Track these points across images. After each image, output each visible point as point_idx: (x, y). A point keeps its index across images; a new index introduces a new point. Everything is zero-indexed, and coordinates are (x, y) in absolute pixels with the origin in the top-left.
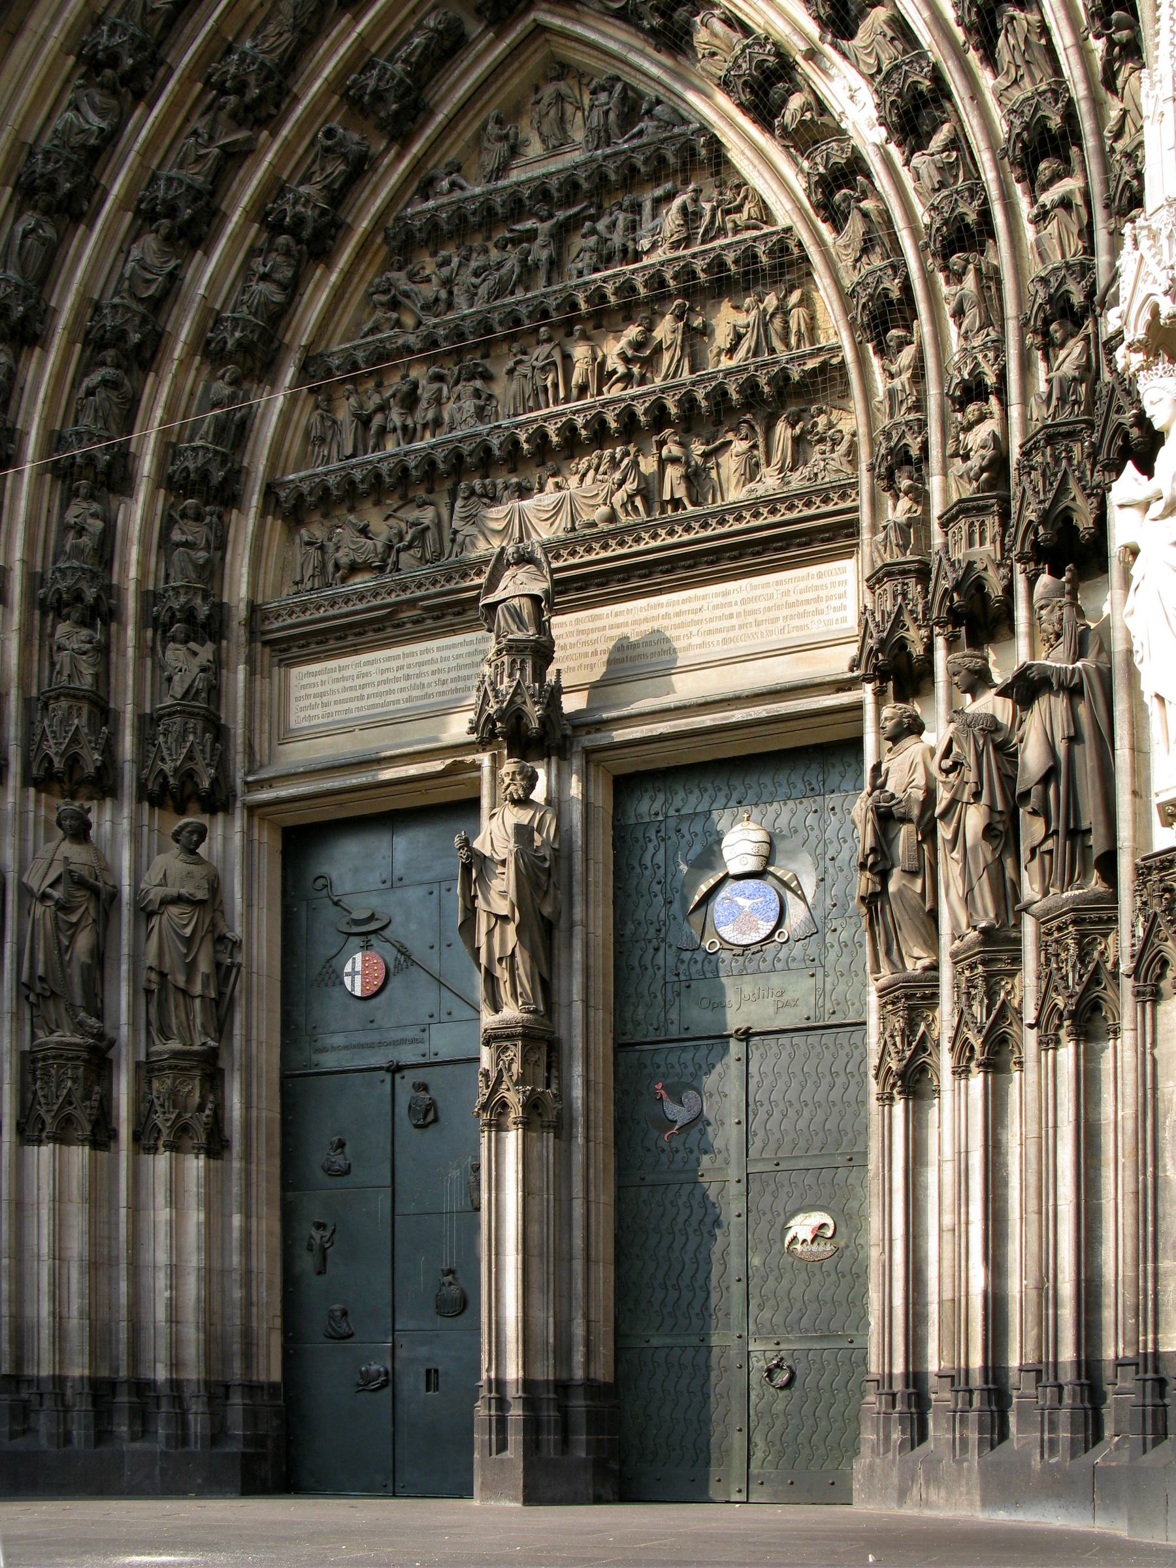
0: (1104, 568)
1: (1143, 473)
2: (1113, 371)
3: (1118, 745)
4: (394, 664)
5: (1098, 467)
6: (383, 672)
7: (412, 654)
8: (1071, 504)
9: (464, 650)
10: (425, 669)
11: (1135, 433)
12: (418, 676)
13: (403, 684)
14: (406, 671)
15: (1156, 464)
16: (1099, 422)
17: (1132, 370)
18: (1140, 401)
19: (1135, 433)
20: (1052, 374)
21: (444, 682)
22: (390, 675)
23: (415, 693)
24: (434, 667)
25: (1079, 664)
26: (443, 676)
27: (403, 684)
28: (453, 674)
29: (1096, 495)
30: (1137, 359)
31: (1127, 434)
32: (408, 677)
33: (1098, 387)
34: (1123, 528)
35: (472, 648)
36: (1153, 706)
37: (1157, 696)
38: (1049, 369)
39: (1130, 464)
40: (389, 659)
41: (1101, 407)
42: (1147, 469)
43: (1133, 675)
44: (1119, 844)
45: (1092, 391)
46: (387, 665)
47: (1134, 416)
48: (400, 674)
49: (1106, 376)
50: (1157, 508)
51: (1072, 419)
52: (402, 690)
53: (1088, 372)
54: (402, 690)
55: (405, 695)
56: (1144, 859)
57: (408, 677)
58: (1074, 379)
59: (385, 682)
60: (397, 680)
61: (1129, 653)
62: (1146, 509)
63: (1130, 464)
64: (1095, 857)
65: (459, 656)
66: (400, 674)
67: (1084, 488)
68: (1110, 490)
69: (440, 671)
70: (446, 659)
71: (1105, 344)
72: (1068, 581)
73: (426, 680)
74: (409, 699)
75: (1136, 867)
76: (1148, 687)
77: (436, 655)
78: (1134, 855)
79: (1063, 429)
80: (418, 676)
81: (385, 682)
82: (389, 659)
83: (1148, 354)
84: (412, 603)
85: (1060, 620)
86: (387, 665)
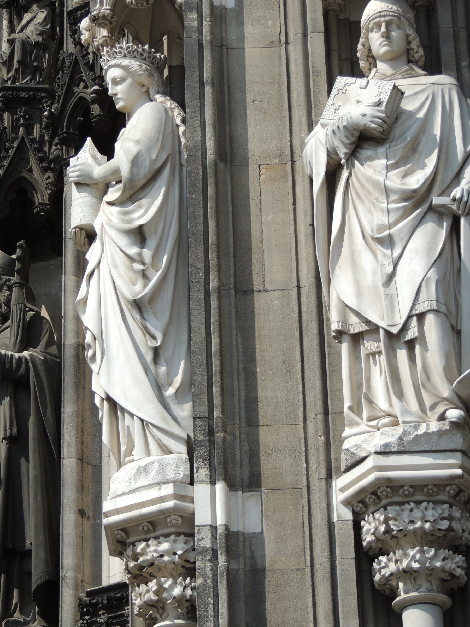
0: (57, 249)
1: (102, 153)
2: (78, 43)
3: (65, 452)
5: (56, 140)
8: (26, 175)
11: (96, 109)
15: (117, 146)
16: (60, 92)
17: (96, 44)
18: (102, 79)
19: (96, 109)
20: (13, 36)
25: (26, 354)
29: (53, 170)
30: (102, 33)
31: (88, 110)
33: (61, 57)
34: (79, 209)
36: (104, 412)
37: (109, 399)
38: (12, 30)
39: (89, 140)
41: (63, 78)
42: (107, 150)
43: (83, 374)
44: (62, 573)
45: (55, 60)
47: (95, 92)
49: (70, 47)
50: (113, 194)
51: (32, 85)
53: (52, 38)
56: (89, 594)
58: (37, 43)
61: (81, 347)
62: (105, 193)
63: (89, 140)
64: (33, 587)
67: (41, 160)
68: (68, 164)
71: (70, 13)
72: (18, 259)
75: (81, 604)
76: (99, 386)
78: (76, 588)
79: (23, 94)
83: (111, 32)
85: (8, 302)
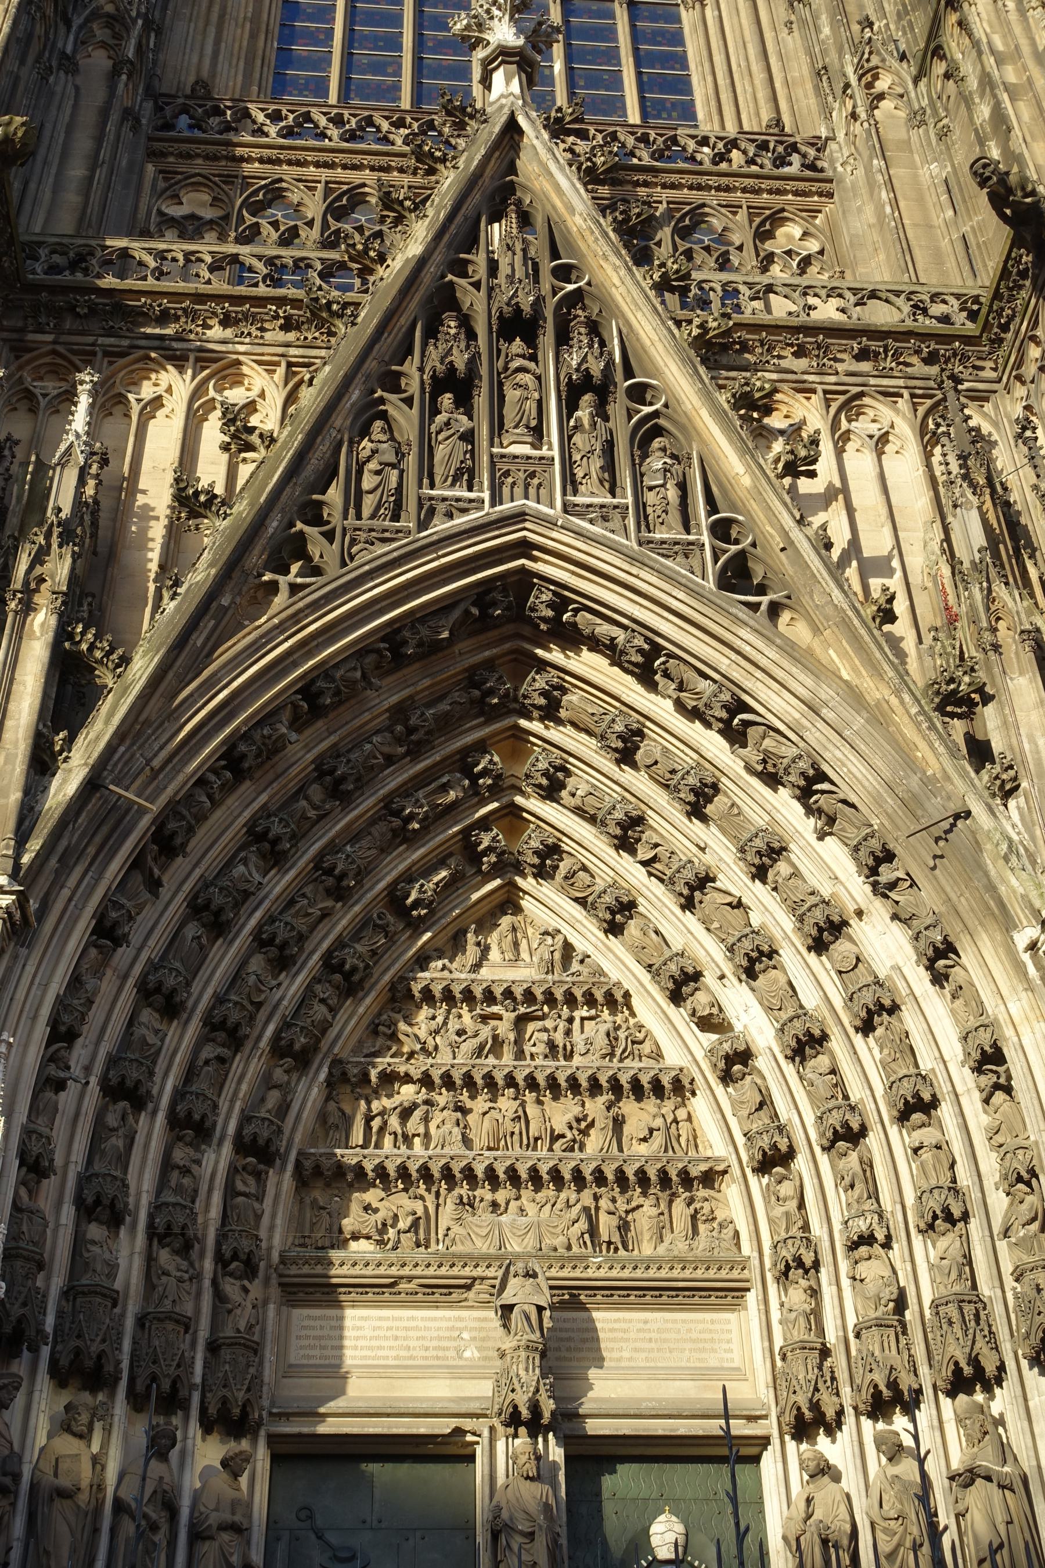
4: (385, 1324)
6: (374, 1329)
7: (401, 1319)
9: (444, 1324)
10: (411, 1333)
12: (405, 1338)
13: (392, 1343)
14: (395, 1333)
21: (427, 1349)
22: (382, 1333)
23: (403, 1353)
24: (420, 1334)
26: (427, 1343)
27: (392, 1343)
28: (435, 1343)
32: (396, 1338)
35: (450, 1324)
40: (380, 1319)
46: (378, 1323)
48: (389, 1334)
52: (391, 1348)
54: (391, 1348)
55: (394, 1353)
57: (396, 1338)
59: (377, 1338)
60: (386, 1338)
65: (439, 1329)
66: (389, 1334)
69: (423, 1338)
70: (429, 1329)
73: (412, 1343)
74: (397, 1358)
77: (421, 1324)
80: (405, 1338)
81: (377, 1338)
82: (380, 1319)
84: (410, 1279)
86: (378, 1323)
